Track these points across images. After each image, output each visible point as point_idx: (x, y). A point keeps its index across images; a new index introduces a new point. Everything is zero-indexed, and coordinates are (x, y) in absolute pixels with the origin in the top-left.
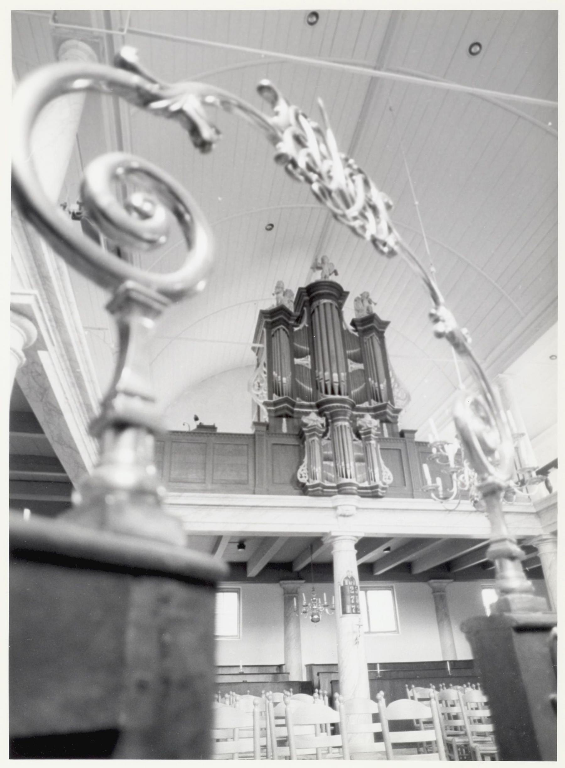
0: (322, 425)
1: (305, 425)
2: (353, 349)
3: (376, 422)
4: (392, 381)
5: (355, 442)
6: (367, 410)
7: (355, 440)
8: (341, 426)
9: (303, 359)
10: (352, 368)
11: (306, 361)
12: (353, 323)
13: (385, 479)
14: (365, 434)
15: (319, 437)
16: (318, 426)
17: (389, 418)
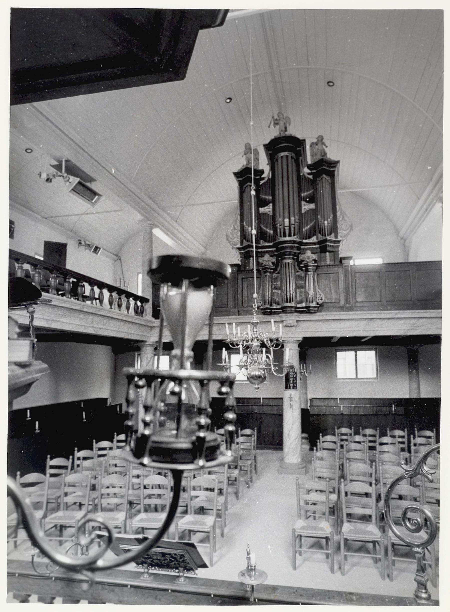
0: (273, 263)
2: (308, 191)
3: (315, 256)
4: (338, 214)
5: (298, 273)
7: (298, 272)
9: (266, 207)
10: (305, 209)
11: (267, 209)
15: (270, 272)
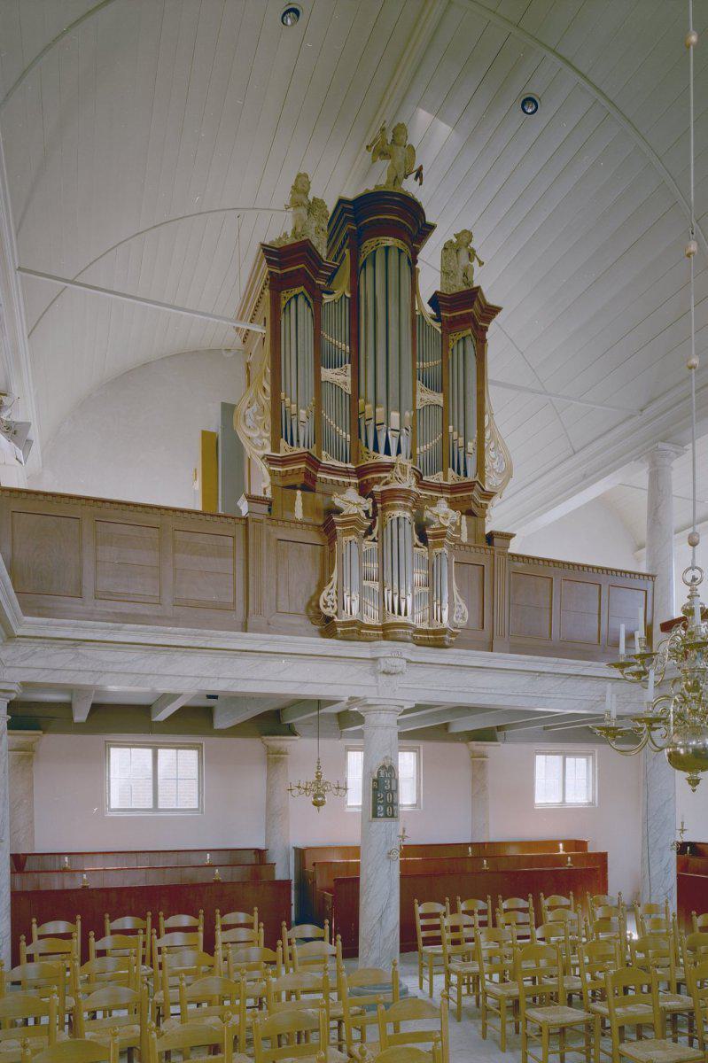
0: (367, 512)
1: (338, 511)
3: (454, 515)
4: (488, 435)
6: (440, 488)
7: (417, 546)
8: (398, 518)
9: (337, 370)
11: (340, 377)
12: (435, 301)
13: (457, 617)
14: (435, 536)
15: (358, 535)
16: (359, 514)
17: (474, 507)
